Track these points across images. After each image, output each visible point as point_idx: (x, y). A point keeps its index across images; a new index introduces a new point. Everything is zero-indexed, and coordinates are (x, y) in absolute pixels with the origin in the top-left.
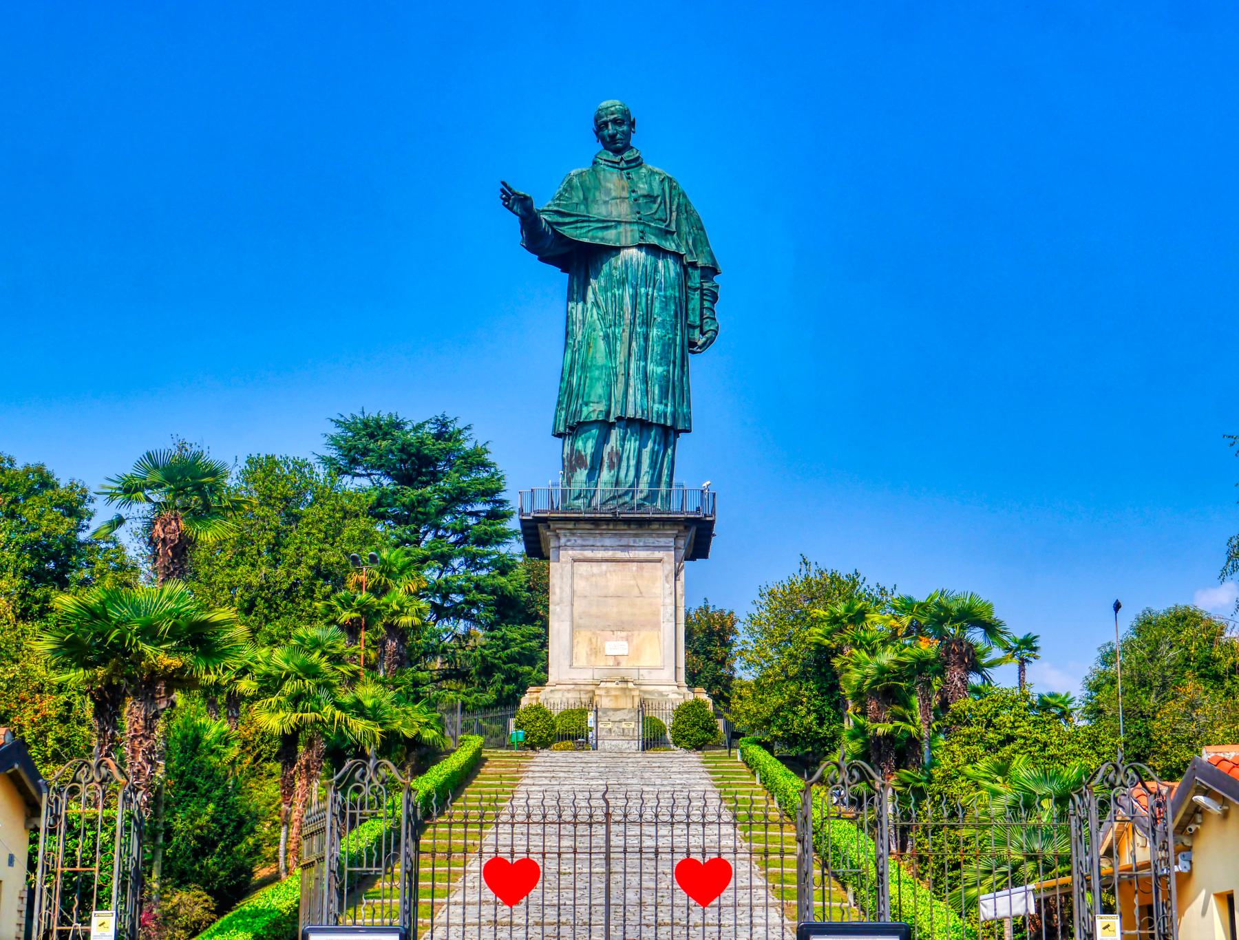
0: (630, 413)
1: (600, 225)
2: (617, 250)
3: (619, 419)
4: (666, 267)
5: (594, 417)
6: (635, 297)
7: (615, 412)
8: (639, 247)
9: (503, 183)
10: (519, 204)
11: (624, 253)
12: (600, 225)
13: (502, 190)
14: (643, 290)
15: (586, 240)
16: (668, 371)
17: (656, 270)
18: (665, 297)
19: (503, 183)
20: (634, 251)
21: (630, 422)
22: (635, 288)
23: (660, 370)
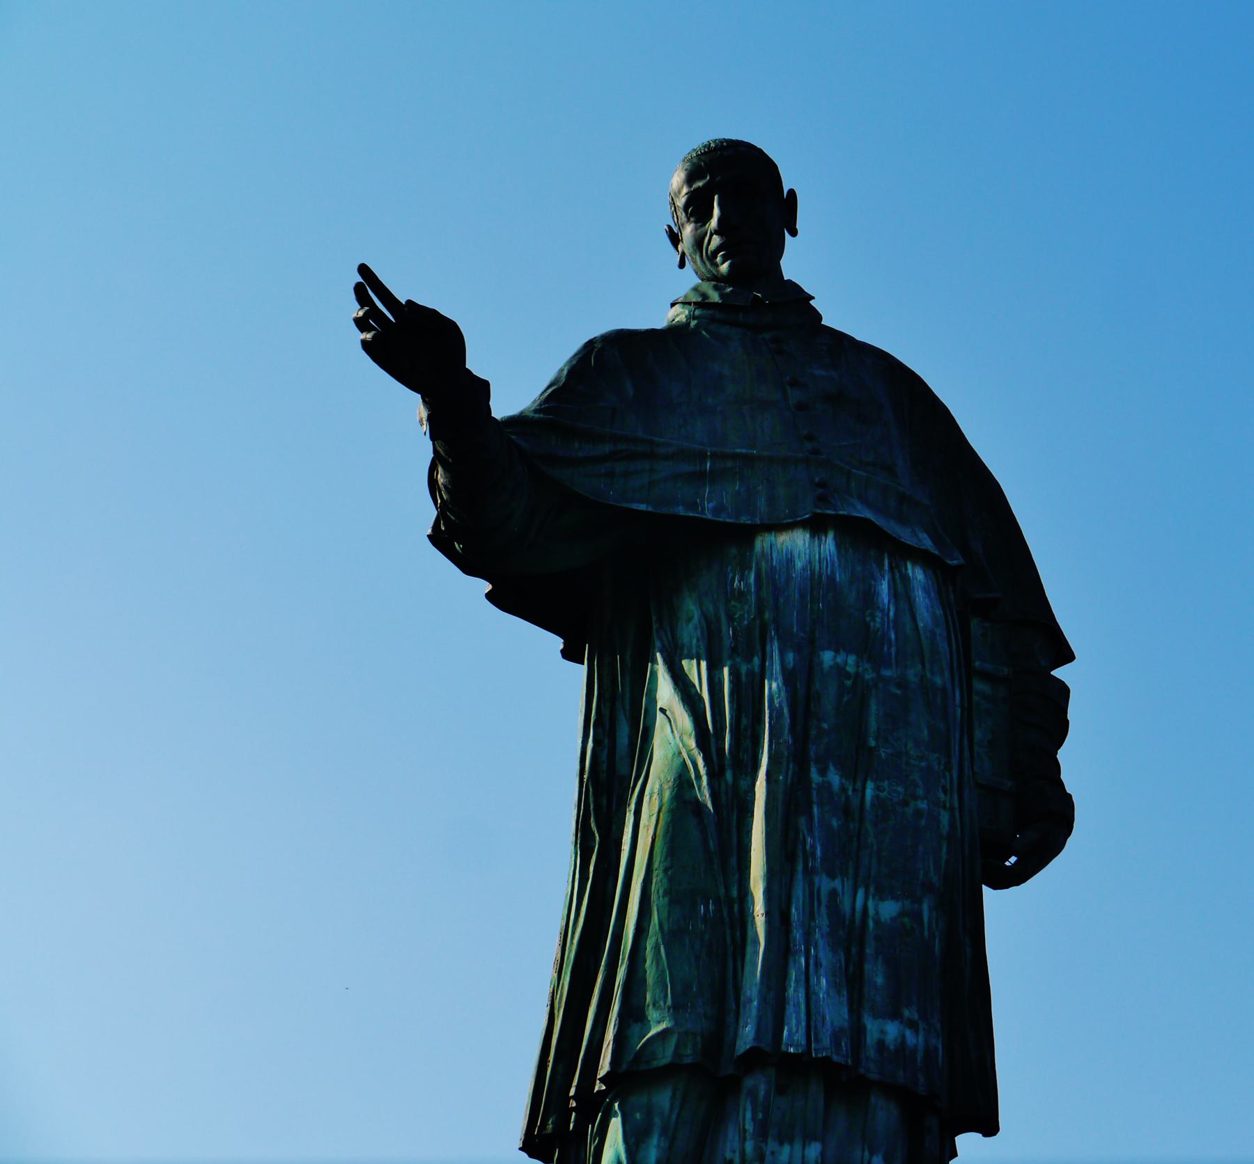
1: (686, 468)
2: (745, 535)
3: (754, 1059)
5: (665, 1055)
6: (801, 683)
7: (747, 1036)
8: (816, 526)
9: (364, 270)
10: (413, 343)
11: (762, 543)
12: (686, 468)
13: (359, 290)
14: (827, 657)
15: (643, 507)
16: (917, 916)
17: (869, 598)
18: (902, 684)
19: (364, 270)
20: (796, 542)
21: (793, 1070)
22: (808, 649)
23: (888, 909)
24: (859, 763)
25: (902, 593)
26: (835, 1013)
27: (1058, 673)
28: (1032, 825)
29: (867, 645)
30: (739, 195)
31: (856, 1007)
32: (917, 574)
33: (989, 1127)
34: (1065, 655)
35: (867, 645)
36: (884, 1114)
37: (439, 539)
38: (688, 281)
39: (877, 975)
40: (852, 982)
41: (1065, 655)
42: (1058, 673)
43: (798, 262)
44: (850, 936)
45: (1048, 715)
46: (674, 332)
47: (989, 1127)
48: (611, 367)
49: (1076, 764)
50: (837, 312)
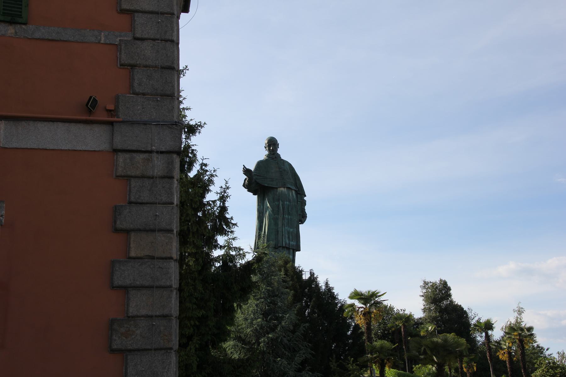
0: (284, 245)
2: (277, 188)
4: (292, 194)
6: (283, 205)
15: (266, 185)
17: (289, 195)
20: (282, 189)
21: (283, 247)
23: (292, 230)
24: (289, 214)
25: (292, 194)
26: (287, 241)
27: (305, 198)
28: (303, 218)
29: (290, 201)
30: (272, 144)
31: (289, 240)
32: (294, 192)
33: (299, 250)
34: (305, 196)
35: (290, 201)
36: (291, 251)
37: (244, 186)
38: (267, 153)
39: (291, 237)
40: (289, 238)
41: (305, 196)
42: (305, 198)
43: (279, 151)
44: (289, 232)
45: (304, 203)
46: (266, 160)
47: (299, 250)
48: (260, 164)
49: (307, 209)
50: (283, 157)
